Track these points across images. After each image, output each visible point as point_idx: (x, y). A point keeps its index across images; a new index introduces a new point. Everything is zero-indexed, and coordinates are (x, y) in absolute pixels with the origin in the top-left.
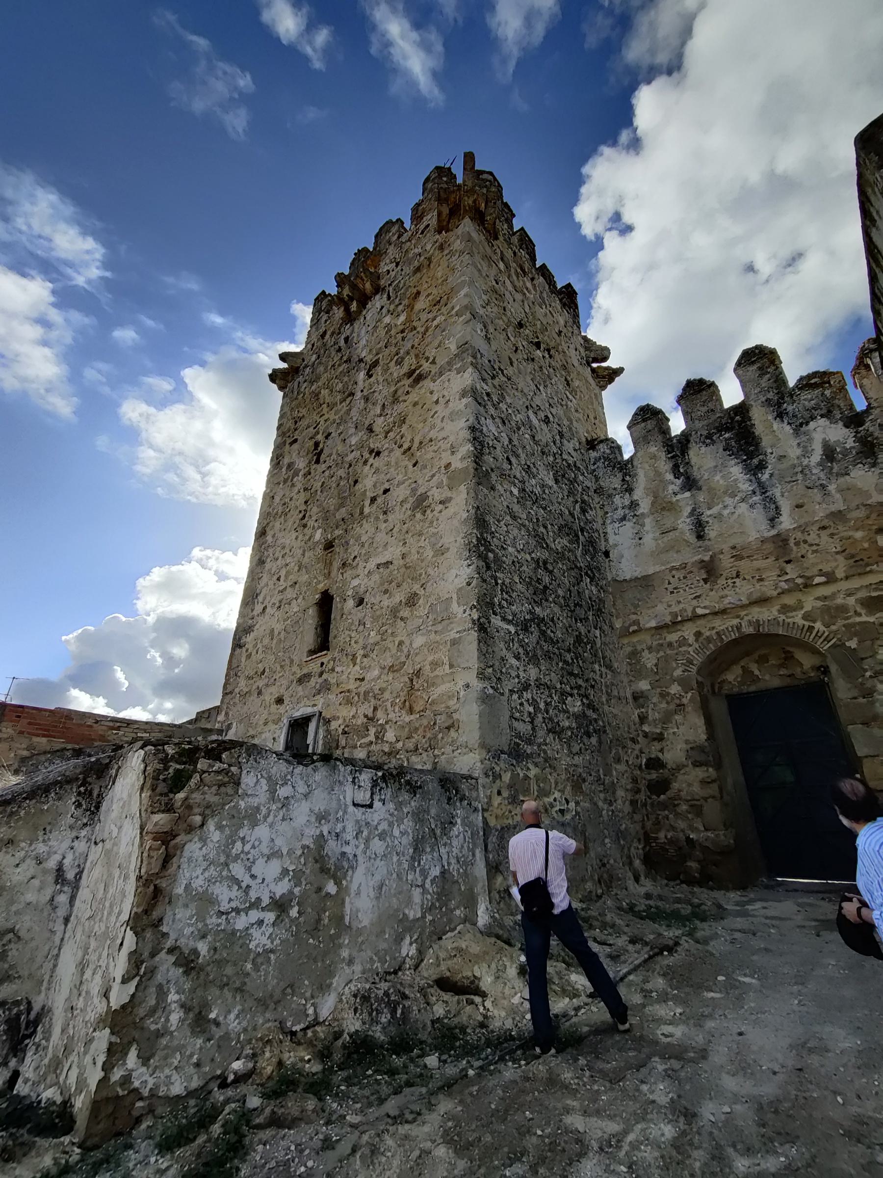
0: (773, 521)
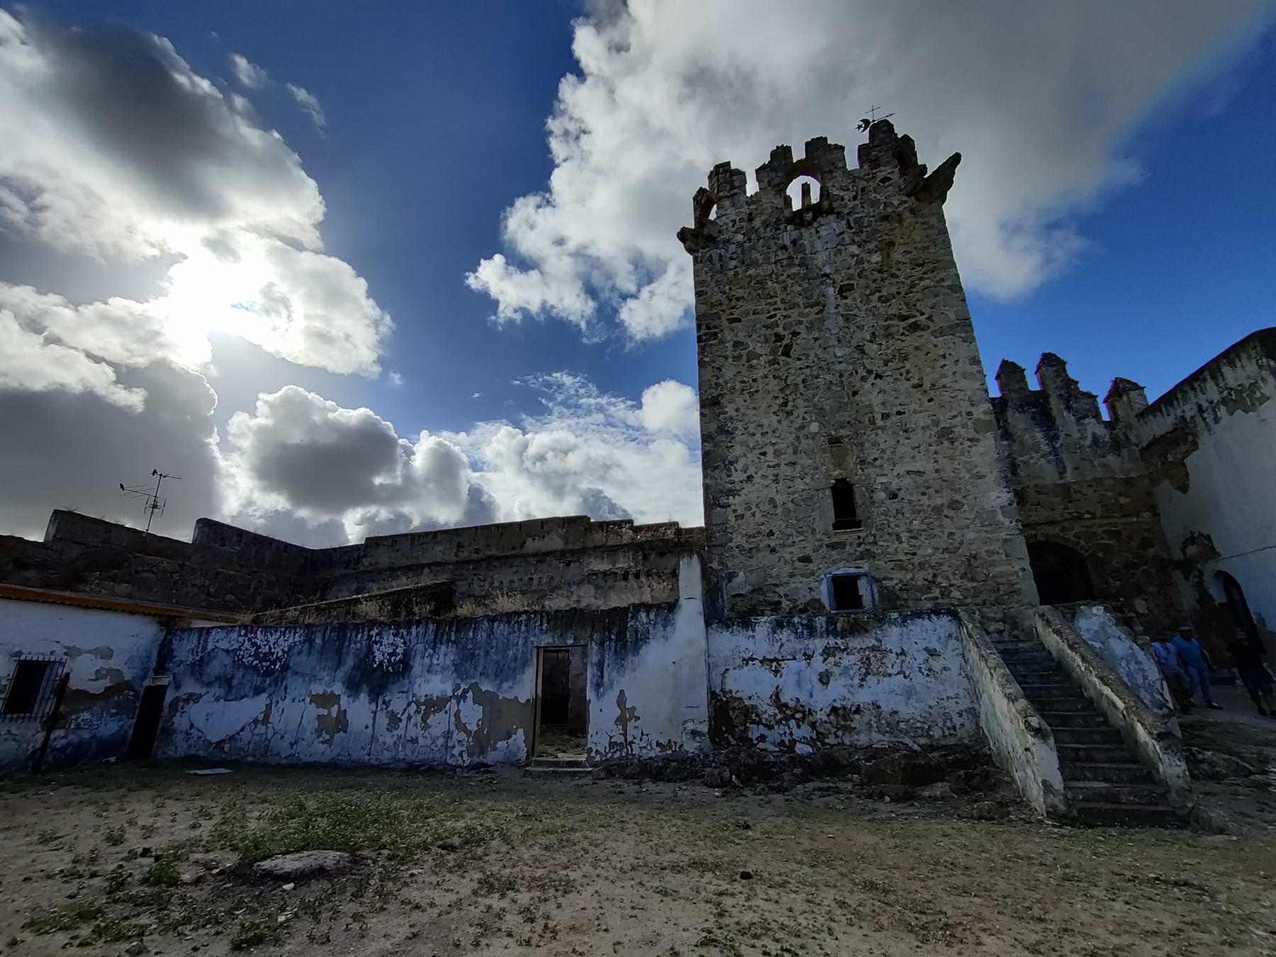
0: (1062, 474)
